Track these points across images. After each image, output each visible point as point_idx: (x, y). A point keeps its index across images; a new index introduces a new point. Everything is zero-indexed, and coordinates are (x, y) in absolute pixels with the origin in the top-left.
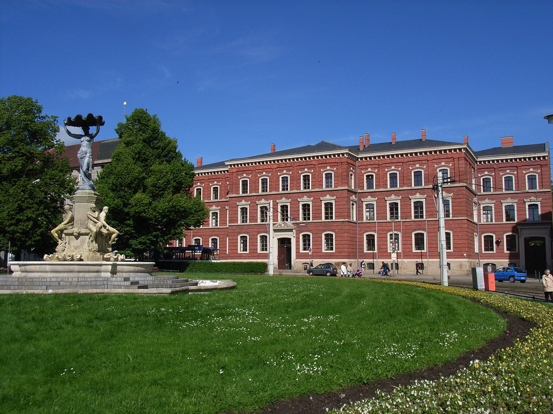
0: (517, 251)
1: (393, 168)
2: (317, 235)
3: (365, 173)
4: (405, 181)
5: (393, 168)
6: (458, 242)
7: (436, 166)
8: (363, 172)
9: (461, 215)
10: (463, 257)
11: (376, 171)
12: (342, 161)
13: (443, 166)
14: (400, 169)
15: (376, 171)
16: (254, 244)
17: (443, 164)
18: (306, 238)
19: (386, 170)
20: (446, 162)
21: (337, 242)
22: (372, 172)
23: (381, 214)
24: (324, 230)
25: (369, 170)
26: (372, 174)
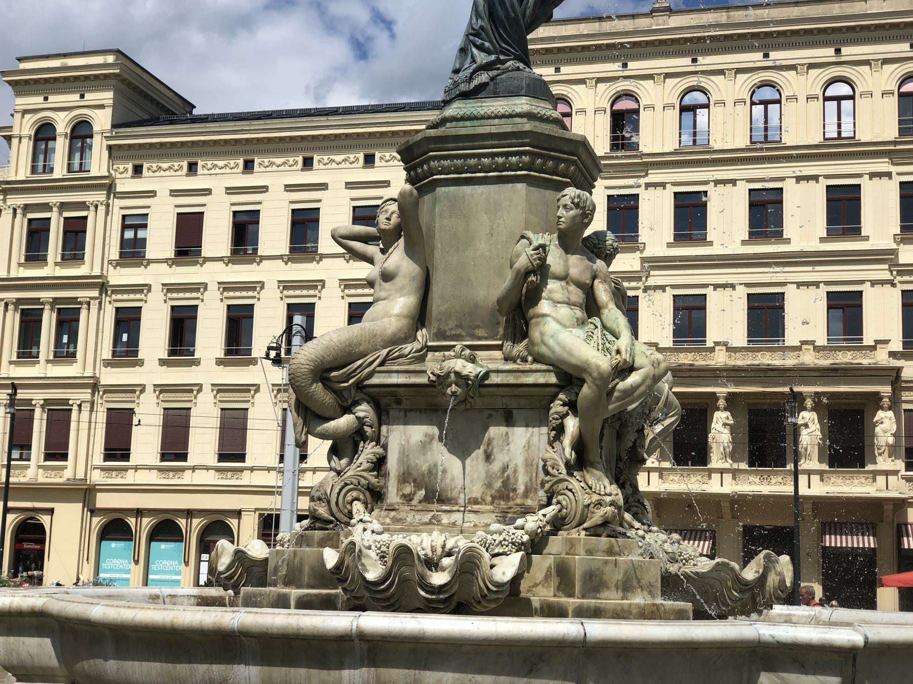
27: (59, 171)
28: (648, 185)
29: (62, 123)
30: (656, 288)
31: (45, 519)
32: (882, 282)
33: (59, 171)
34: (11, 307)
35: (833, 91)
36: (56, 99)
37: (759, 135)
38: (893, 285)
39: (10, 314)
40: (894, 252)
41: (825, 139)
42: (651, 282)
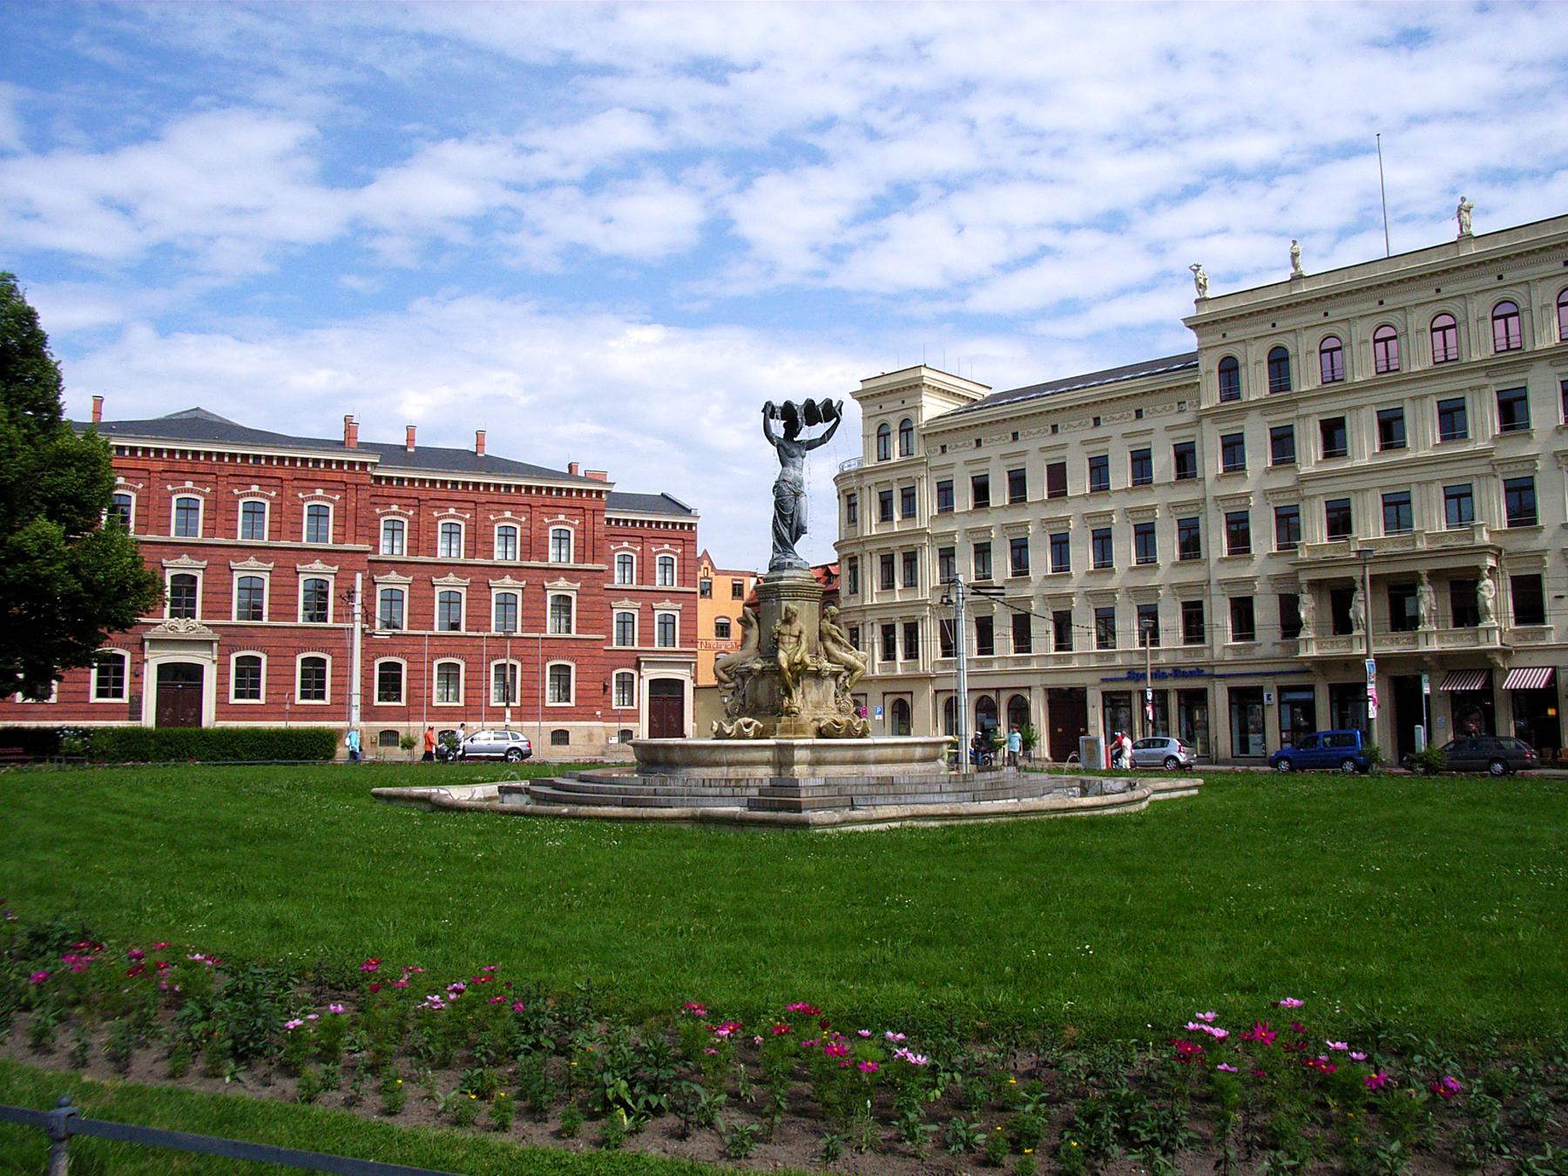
0: (635, 707)
1: (452, 511)
2: (282, 661)
3: (383, 515)
4: (479, 546)
5: (452, 511)
6: (585, 685)
7: (546, 520)
8: (378, 511)
9: (595, 629)
10: (593, 717)
11: (411, 513)
12: (358, 481)
13: (561, 523)
14: (468, 516)
15: (411, 513)
16: (281, 682)
17: (562, 517)
18: (248, 670)
19: (436, 514)
20: (567, 516)
21: (338, 678)
22: (400, 514)
23: (284, 608)
24: (301, 647)
25: (395, 508)
26: (401, 519)
27: (896, 457)
28: (1298, 417)
29: (895, 427)
30: (1310, 497)
31: (907, 698)
32: (1487, 475)
33: (896, 457)
34: (874, 555)
35: (1439, 323)
36: (887, 407)
37: (1382, 368)
38: (1495, 476)
39: (874, 559)
40: (1491, 450)
41: (1435, 363)
42: (1307, 492)
